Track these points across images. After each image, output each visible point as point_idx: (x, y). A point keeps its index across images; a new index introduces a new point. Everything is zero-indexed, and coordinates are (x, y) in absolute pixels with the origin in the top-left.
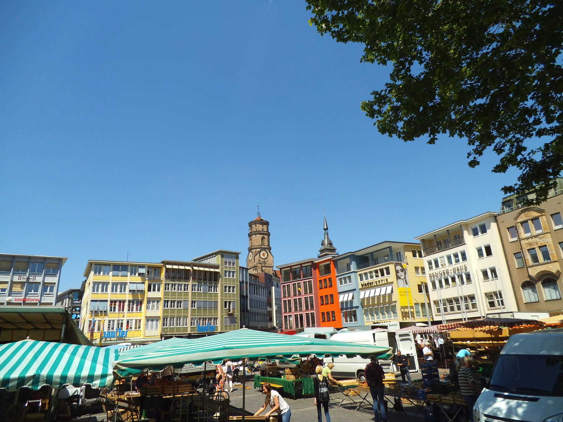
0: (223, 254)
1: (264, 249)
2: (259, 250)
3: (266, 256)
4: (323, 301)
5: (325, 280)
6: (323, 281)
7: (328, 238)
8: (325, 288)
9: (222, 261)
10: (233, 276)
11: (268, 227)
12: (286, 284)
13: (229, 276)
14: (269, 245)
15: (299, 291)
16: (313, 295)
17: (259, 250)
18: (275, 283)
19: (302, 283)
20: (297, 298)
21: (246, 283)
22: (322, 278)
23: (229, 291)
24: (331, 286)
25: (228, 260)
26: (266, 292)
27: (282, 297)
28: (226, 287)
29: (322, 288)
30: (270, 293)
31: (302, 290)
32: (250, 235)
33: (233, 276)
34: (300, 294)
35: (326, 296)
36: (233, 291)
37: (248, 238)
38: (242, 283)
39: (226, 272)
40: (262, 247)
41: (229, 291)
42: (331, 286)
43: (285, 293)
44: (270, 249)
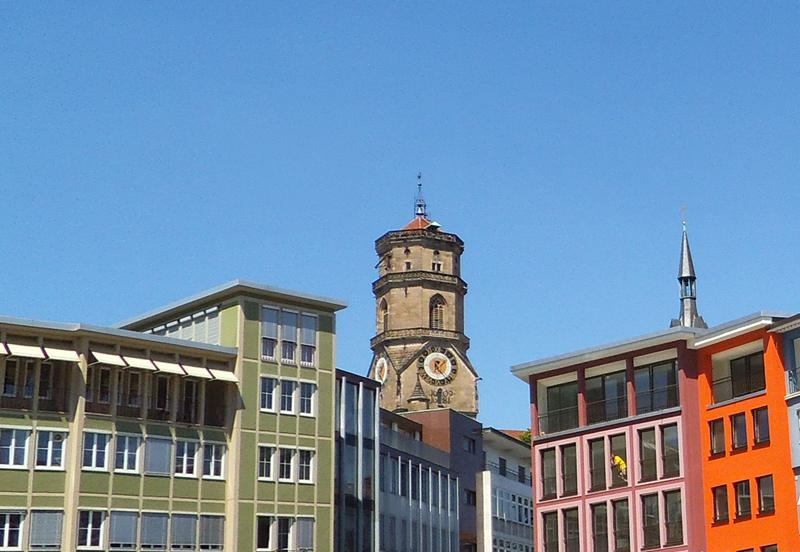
0: (255, 302)
1: (441, 344)
2: (418, 346)
3: (448, 371)
4: (724, 507)
5: (737, 420)
6: (727, 424)
7: (694, 312)
8: (735, 451)
9: (248, 336)
10: (305, 406)
11: (457, 260)
12: (556, 444)
13: (286, 403)
14: (459, 331)
15: (615, 468)
16: (682, 485)
17: (418, 346)
18: (492, 458)
19: (631, 434)
20: (608, 498)
21: (369, 444)
22: (725, 412)
23: (284, 471)
24: (763, 442)
25: (280, 333)
26: (453, 491)
27: (539, 496)
28: (266, 453)
29: (722, 454)
30: (472, 498)
31: (632, 467)
32: (381, 289)
33: (305, 406)
34: (620, 481)
35: (741, 487)
36: (304, 473)
37: (372, 301)
38: (345, 444)
39: (268, 384)
40: (432, 334)
41: (284, 471)
42: (763, 442)
43: (549, 483)
44: (463, 344)
